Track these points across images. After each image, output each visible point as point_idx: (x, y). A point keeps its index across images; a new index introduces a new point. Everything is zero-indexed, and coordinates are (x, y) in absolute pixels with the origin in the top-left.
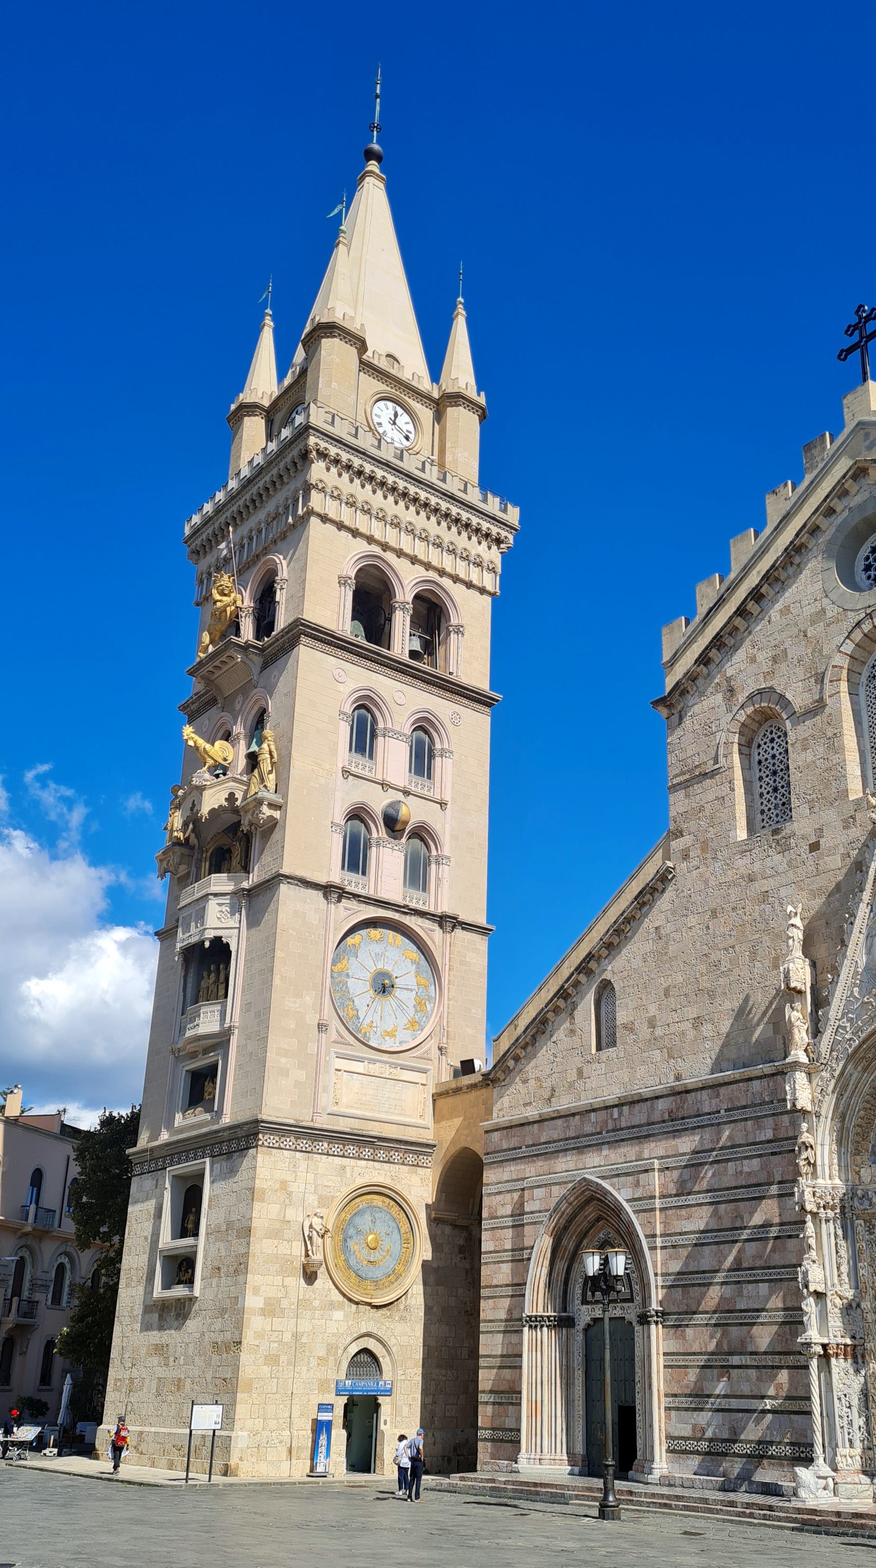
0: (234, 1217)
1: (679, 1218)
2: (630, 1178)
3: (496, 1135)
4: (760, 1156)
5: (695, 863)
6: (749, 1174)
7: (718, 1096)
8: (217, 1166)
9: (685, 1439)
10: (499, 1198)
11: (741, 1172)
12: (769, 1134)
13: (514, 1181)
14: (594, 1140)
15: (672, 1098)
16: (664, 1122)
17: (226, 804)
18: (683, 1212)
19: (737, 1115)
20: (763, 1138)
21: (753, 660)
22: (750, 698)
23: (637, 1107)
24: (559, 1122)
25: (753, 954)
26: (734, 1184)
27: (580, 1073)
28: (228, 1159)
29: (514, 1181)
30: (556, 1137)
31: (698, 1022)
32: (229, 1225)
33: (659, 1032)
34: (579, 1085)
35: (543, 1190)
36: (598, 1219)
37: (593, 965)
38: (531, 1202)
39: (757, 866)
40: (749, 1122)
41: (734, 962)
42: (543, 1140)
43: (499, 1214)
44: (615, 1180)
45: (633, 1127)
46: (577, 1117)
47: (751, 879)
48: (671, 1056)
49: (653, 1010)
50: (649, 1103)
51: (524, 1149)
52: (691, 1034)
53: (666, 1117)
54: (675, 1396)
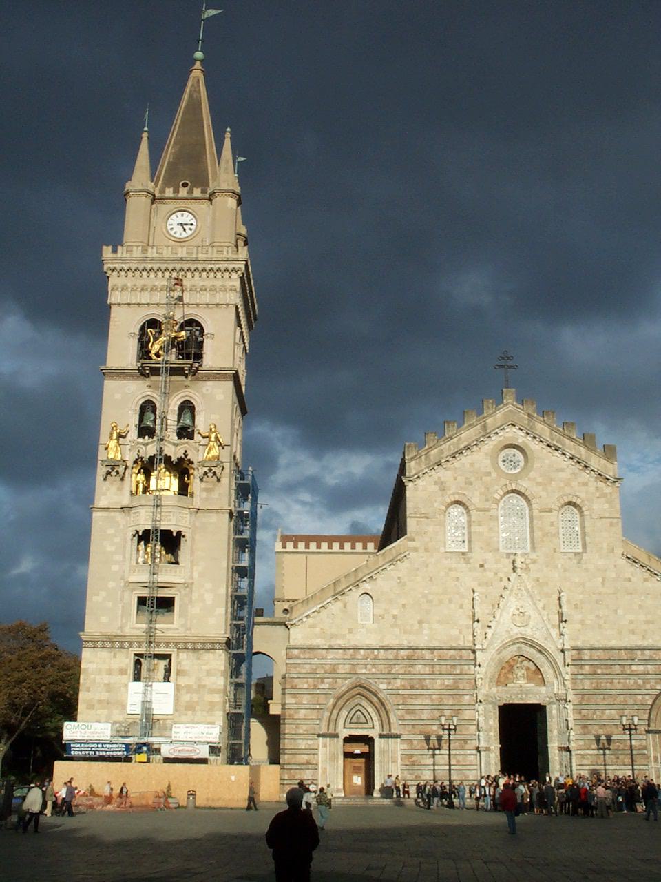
0: (203, 683)
1: (412, 698)
2: (385, 681)
3: (296, 652)
4: (453, 679)
5: (422, 555)
6: (447, 686)
7: (433, 653)
8: (183, 655)
9: (412, 780)
10: (297, 680)
11: (444, 684)
12: (458, 672)
13: (309, 673)
14: (363, 662)
15: (408, 651)
16: (404, 660)
17: (183, 456)
18: (413, 697)
19: (442, 662)
20: (455, 673)
21: (455, 479)
22: (453, 494)
23: (390, 651)
24: (340, 651)
25: (450, 601)
26: (440, 688)
27: (350, 631)
28: (194, 652)
29: (309, 673)
30: (338, 657)
31: (420, 622)
32: (200, 686)
33: (399, 622)
34: (348, 636)
35: (331, 680)
36: (359, 694)
37: (360, 584)
38: (323, 684)
39: (454, 566)
40: (448, 666)
41: (441, 601)
42: (329, 658)
43: (298, 687)
44: (376, 680)
45: (386, 659)
46: (352, 651)
47: (451, 570)
48: (405, 632)
49: (395, 612)
50: (395, 651)
51: (316, 660)
52: (416, 626)
53: (405, 658)
54: (406, 765)
